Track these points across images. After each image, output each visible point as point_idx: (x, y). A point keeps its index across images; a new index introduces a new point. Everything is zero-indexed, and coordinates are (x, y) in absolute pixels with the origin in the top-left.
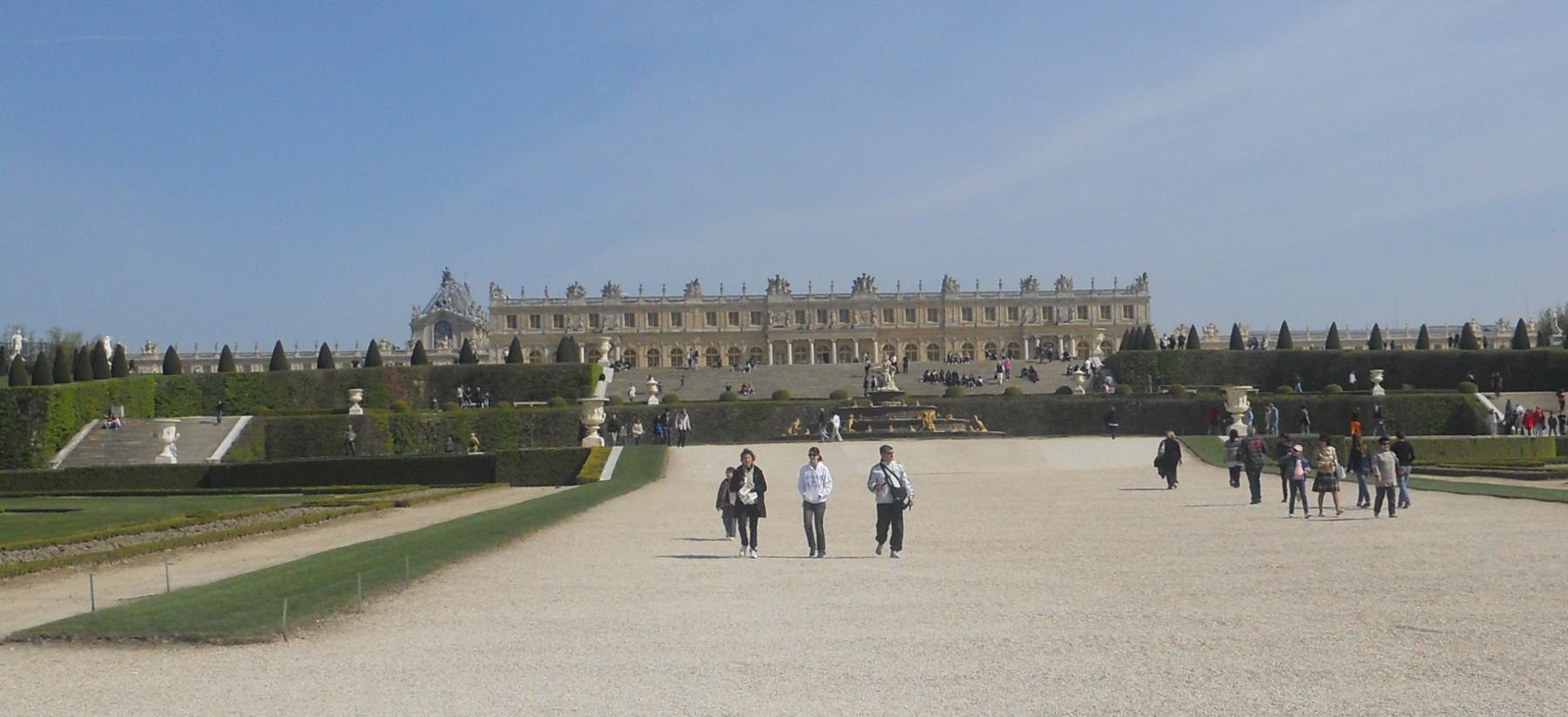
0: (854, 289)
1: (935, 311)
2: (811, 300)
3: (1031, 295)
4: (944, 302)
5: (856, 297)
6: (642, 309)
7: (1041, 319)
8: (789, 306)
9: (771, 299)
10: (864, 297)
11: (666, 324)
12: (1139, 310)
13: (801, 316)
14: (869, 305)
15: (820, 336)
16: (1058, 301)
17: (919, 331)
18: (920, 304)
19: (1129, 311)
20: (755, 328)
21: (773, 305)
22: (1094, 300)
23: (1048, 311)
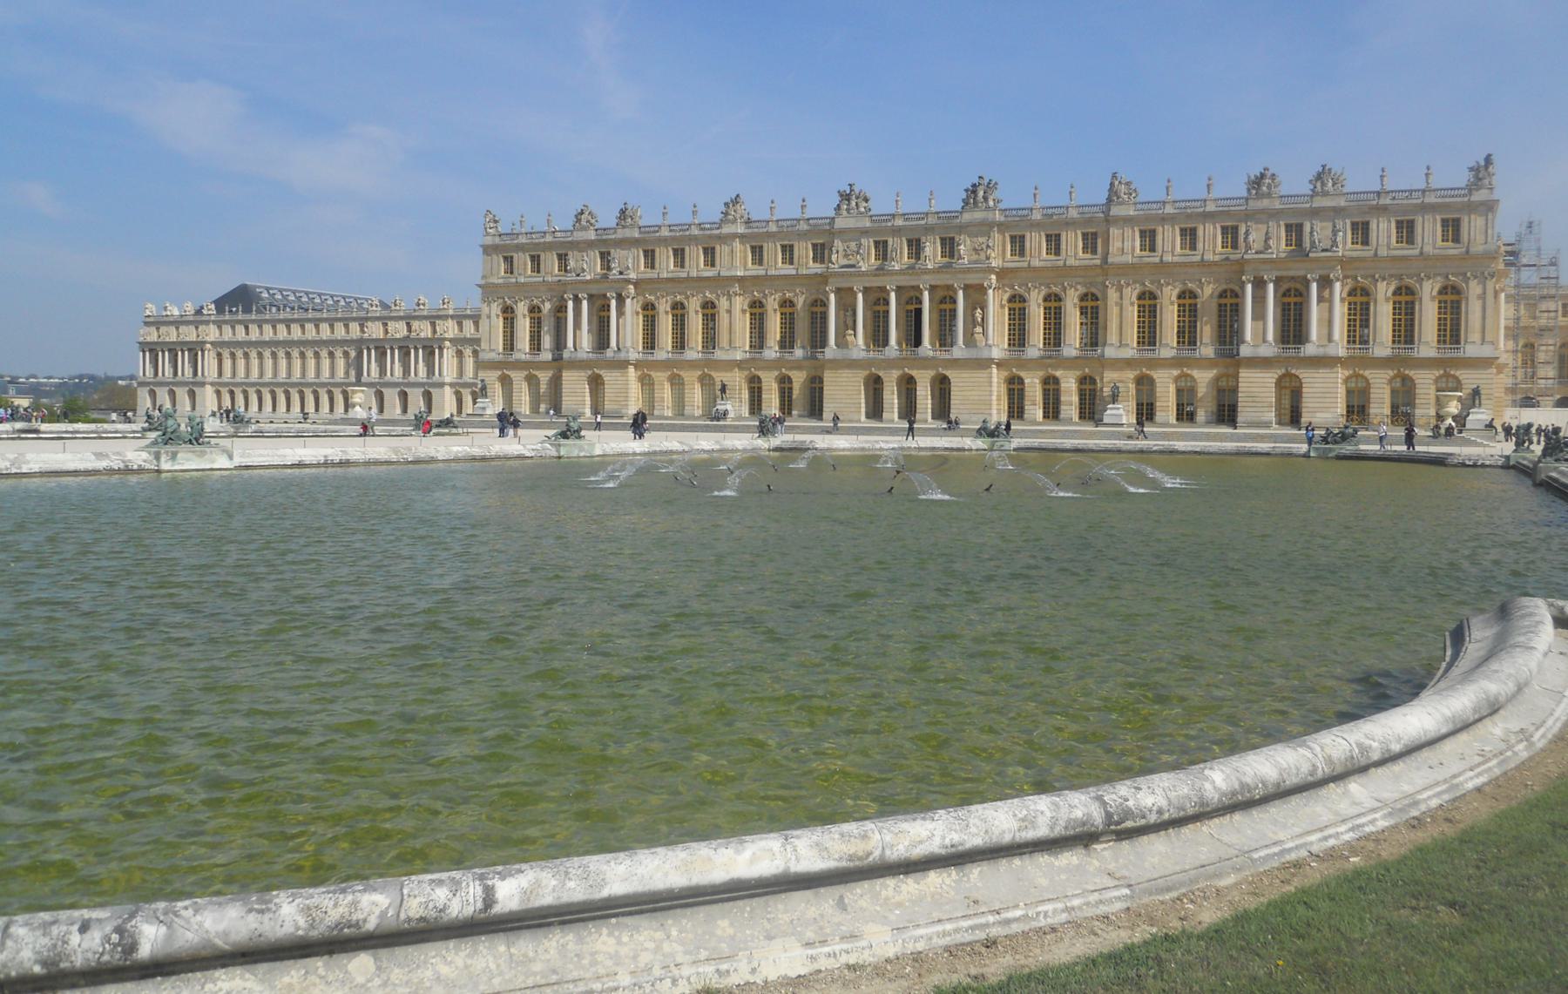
0: (966, 202)
1: (1095, 235)
2: (899, 222)
3: (1265, 203)
4: (1109, 221)
5: (967, 217)
6: (664, 241)
7: (1280, 246)
8: (865, 232)
9: (840, 223)
10: (978, 215)
11: (696, 264)
12: (1473, 227)
13: (882, 249)
14: (986, 228)
15: (905, 281)
16: (1315, 213)
17: (1066, 271)
18: (1069, 224)
19: (1452, 228)
20: (816, 268)
21: (842, 232)
22: (1382, 210)
23: (1295, 231)
